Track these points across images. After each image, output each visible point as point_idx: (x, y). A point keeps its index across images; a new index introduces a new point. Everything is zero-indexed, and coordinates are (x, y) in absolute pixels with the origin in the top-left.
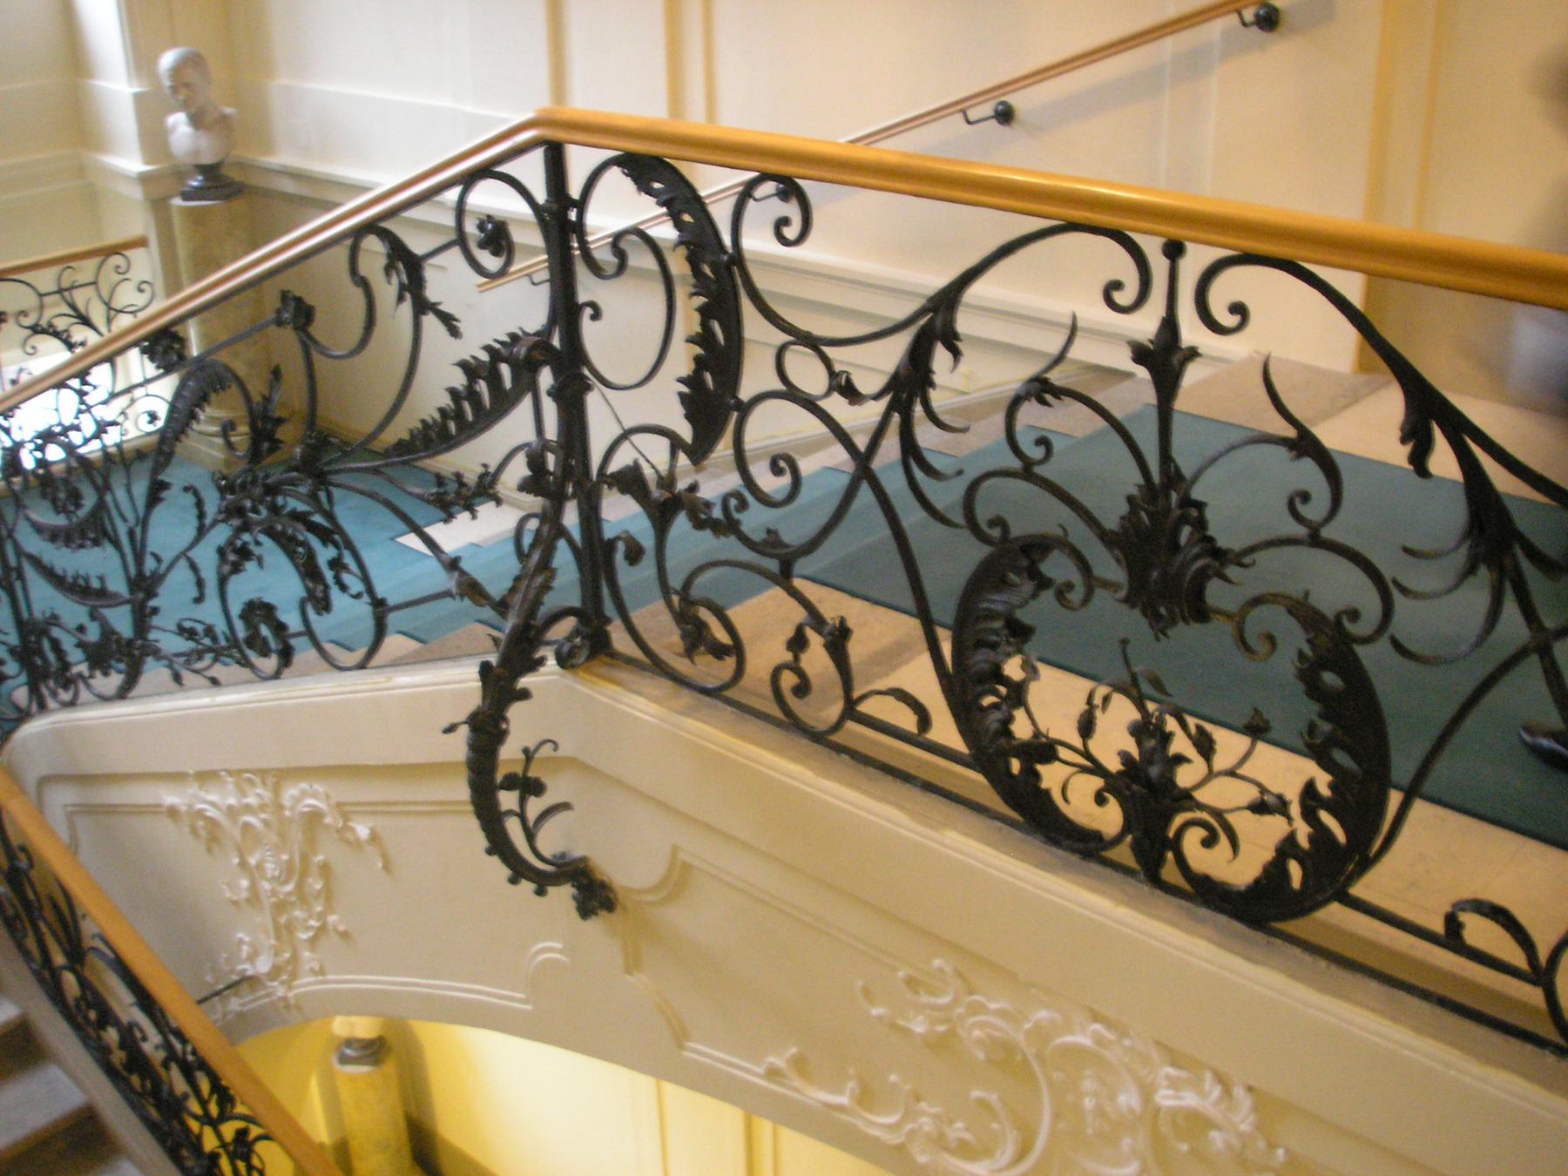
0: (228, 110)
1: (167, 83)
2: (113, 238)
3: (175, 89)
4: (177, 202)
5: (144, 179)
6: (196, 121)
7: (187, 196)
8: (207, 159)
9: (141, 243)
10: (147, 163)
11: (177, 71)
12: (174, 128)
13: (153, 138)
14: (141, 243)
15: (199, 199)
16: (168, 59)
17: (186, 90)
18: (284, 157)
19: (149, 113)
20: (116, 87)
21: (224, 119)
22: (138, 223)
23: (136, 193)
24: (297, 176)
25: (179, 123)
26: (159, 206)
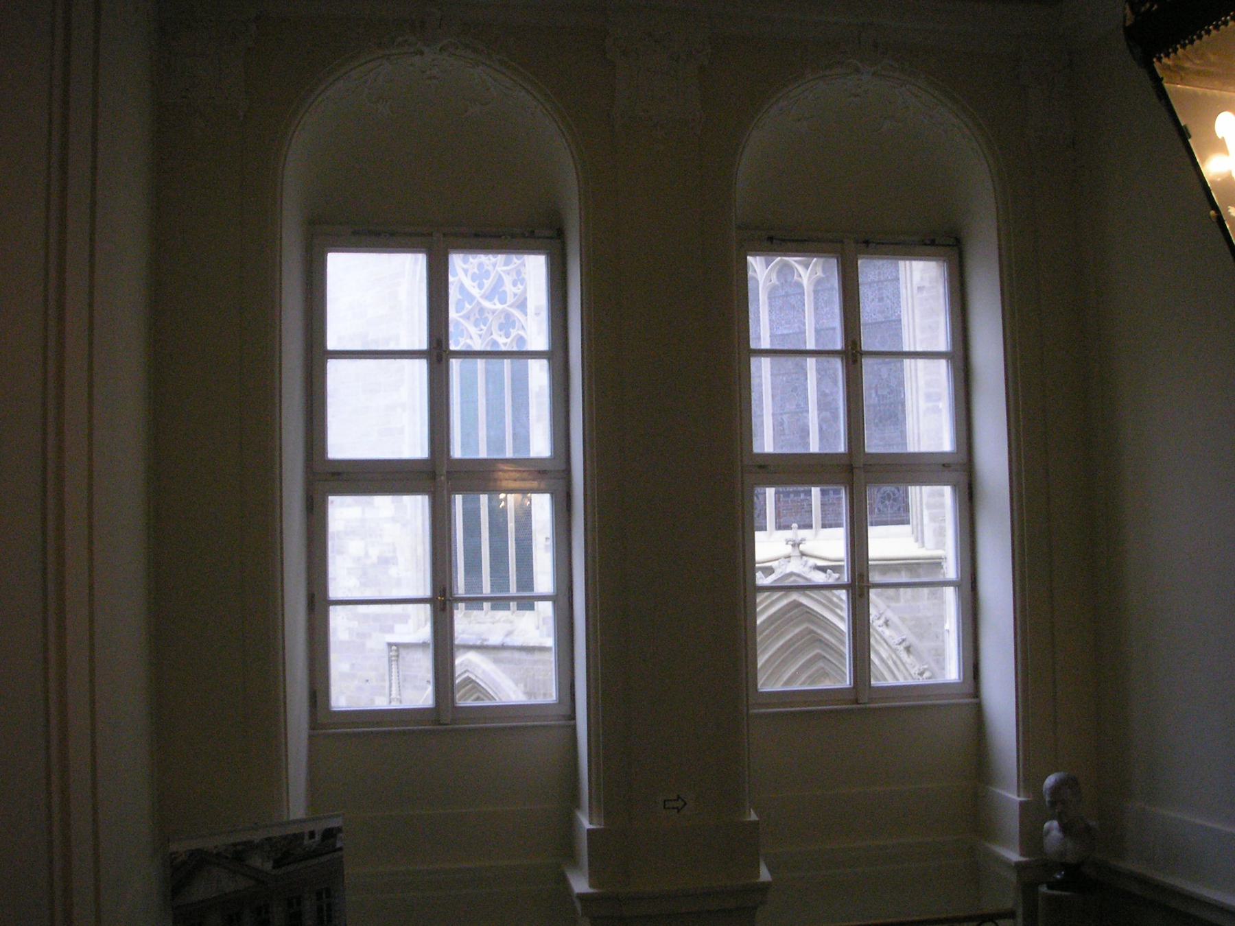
0: (1093, 823)
1: (1047, 799)
2: (988, 908)
3: (1053, 804)
4: (1043, 889)
5: (1019, 866)
6: (1064, 828)
7: (1050, 887)
8: (1070, 859)
9: (1011, 915)
10: (1022, 855)
11: (1056, 789)
12: (1048, 831)
13: (1031, 838)
14: (1011, 915)
15: (1062, 890)
16: (1050, 780)
17: (1060, 803)
18: (1131, 865)
19: (1031, 815)
20: (1010, 795)
21: (1088, 829)
22: (1009, 899)
23: (1013, 877)
24: (1143, 881)
25: (1052, 825)
26: (1028, 889)
